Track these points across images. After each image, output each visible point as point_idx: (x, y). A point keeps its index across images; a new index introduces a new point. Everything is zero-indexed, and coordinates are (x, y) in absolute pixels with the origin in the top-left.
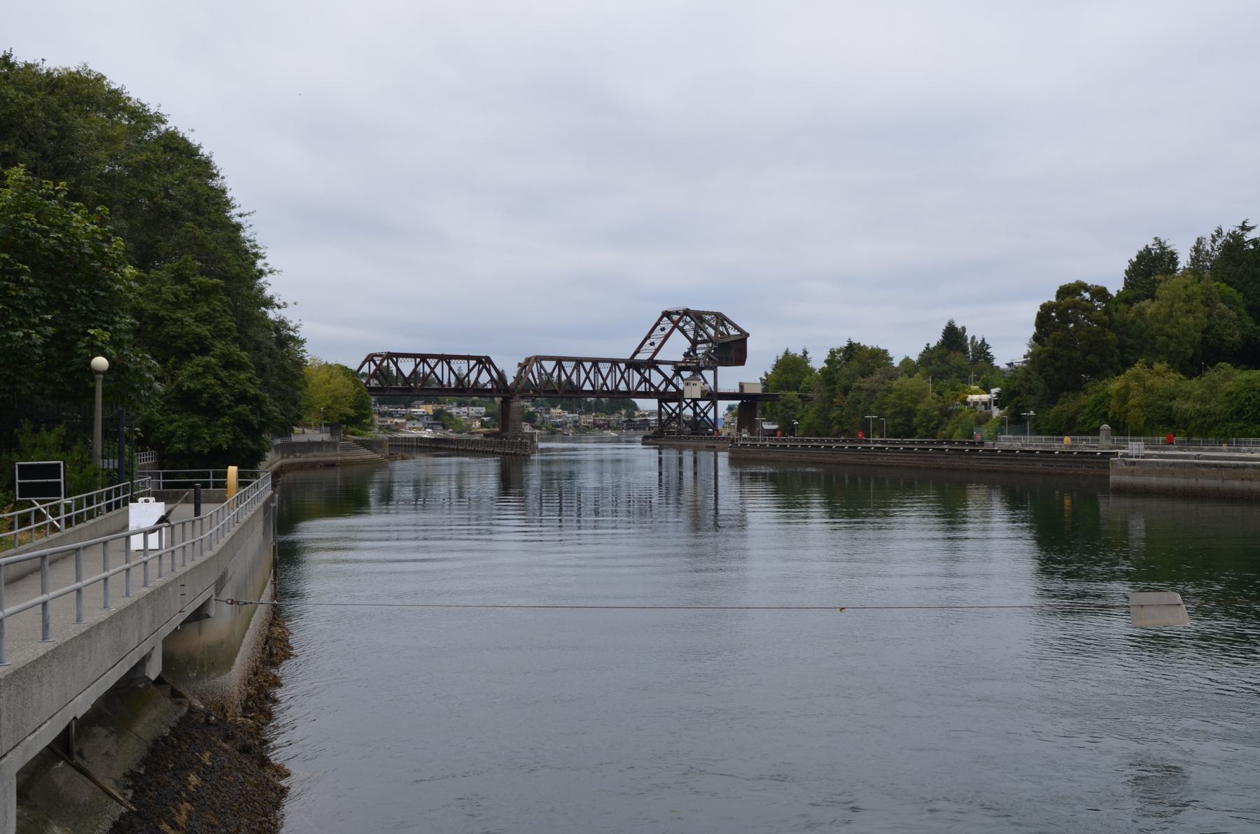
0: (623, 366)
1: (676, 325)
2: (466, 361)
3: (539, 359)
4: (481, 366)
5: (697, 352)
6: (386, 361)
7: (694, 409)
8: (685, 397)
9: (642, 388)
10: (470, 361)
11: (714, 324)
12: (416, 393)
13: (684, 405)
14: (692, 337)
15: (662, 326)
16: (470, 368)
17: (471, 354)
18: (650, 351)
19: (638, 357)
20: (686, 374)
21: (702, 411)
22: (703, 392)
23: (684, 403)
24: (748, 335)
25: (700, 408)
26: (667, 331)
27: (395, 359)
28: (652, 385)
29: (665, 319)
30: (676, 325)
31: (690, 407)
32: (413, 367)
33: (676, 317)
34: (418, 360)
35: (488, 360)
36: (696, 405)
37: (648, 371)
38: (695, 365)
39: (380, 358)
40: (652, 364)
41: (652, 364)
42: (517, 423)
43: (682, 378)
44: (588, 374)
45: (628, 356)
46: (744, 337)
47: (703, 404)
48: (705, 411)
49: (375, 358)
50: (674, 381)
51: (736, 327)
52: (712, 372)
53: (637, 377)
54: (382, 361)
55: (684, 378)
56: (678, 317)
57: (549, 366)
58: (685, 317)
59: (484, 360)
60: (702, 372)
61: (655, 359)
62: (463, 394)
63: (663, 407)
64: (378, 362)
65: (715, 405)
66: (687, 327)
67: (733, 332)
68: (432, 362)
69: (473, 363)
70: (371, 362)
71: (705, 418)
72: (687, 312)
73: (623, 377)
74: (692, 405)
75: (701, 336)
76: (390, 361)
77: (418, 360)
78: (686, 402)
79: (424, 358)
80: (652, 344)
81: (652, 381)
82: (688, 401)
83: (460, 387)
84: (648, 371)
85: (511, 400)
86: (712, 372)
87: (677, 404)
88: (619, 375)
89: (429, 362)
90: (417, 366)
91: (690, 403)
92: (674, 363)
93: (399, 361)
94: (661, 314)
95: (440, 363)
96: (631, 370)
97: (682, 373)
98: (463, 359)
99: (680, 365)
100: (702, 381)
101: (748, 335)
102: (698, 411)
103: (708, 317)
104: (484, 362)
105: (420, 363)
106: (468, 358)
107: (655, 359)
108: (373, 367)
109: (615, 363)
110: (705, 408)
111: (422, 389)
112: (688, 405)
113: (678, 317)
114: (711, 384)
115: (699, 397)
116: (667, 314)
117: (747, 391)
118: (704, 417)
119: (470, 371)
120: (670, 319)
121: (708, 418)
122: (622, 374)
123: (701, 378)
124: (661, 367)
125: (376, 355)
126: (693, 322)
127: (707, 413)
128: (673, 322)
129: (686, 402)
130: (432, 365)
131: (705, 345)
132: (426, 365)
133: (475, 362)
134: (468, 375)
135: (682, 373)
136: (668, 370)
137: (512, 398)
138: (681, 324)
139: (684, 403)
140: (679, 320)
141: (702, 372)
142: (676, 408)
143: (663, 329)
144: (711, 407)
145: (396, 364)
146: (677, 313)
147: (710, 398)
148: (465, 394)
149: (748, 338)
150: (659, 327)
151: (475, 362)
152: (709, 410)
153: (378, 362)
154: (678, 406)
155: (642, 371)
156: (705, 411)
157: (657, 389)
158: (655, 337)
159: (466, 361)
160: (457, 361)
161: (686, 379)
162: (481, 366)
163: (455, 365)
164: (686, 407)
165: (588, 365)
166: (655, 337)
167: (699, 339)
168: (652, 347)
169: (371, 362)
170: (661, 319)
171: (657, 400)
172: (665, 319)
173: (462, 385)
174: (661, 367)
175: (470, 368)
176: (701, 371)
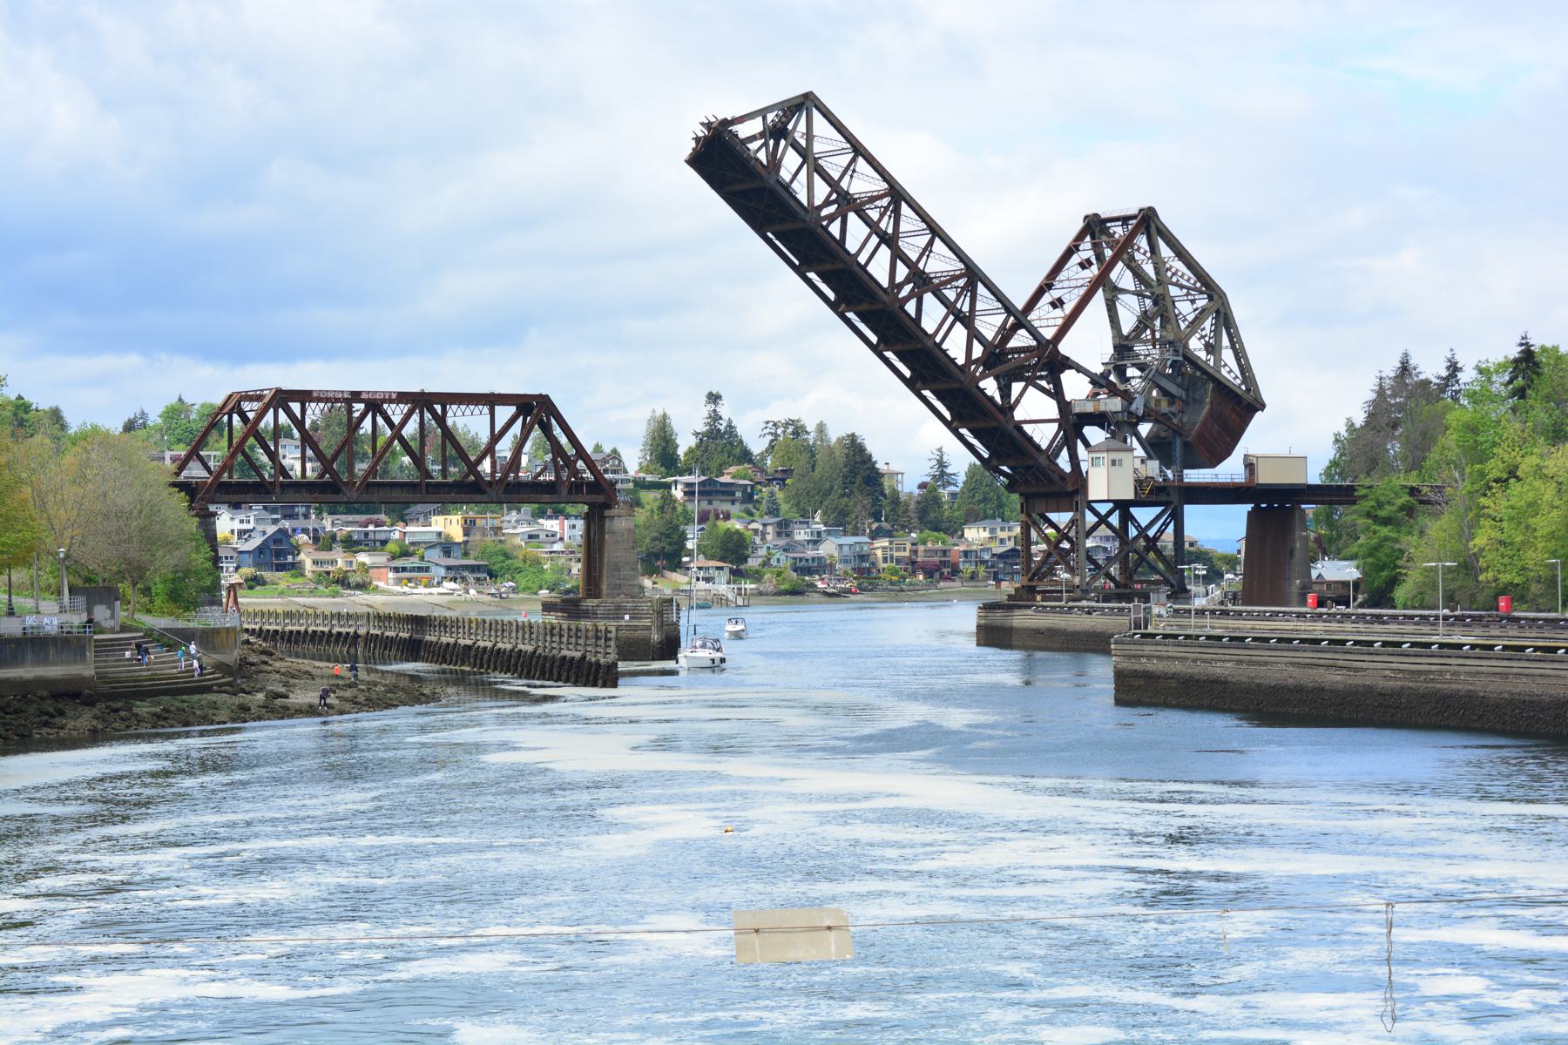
6: (270, 415)
7: (1121, 533)
8: (1091, 497)
10: (497, 408)
12: (353, 495)
16: (498, 429)
17: (497, 391)
21: (1142, 531)
22: (1139, 483)
23: (1088, 513)
25: (1138, 526)
36: (1126, 518)
39: (256, 405)
42: (626, 572)
43: (1087, 444)
47: (1143, 515)
48: (1151, 533)
49: (246, 406)
54: (261, 414)
55: (1092, 443)
62: (478, 497)
65: (1177, 518)
69: (504, 413)
71: (1152, 555)
74: (1114, 520)
76: (280, 410)
78: (1096, 513)
82: (1103, 509)
83: (472, 478)
85: (607, 513)
89: (389, 412)
91: (1110, 513)
94: (1080, 225)
106: (491, 400)
111: (368, 486)
115: (1130, 495)
117: (1265, 477)
118: (1147, 549)
121: (1159, 553)
130: (396, 420)
133: (512, 410)
137: (609, 507)
144: (1166, 524)
147: (1163, 498)
148: (485, 498)
151: (512, 410)
152: (1161, 531)
154: (1073, 522)
156: (1151, 533)
159: (486, 410)
160: (472, 407)
173: (478, 475)
175: (498, 429)
176: (1137, 424)
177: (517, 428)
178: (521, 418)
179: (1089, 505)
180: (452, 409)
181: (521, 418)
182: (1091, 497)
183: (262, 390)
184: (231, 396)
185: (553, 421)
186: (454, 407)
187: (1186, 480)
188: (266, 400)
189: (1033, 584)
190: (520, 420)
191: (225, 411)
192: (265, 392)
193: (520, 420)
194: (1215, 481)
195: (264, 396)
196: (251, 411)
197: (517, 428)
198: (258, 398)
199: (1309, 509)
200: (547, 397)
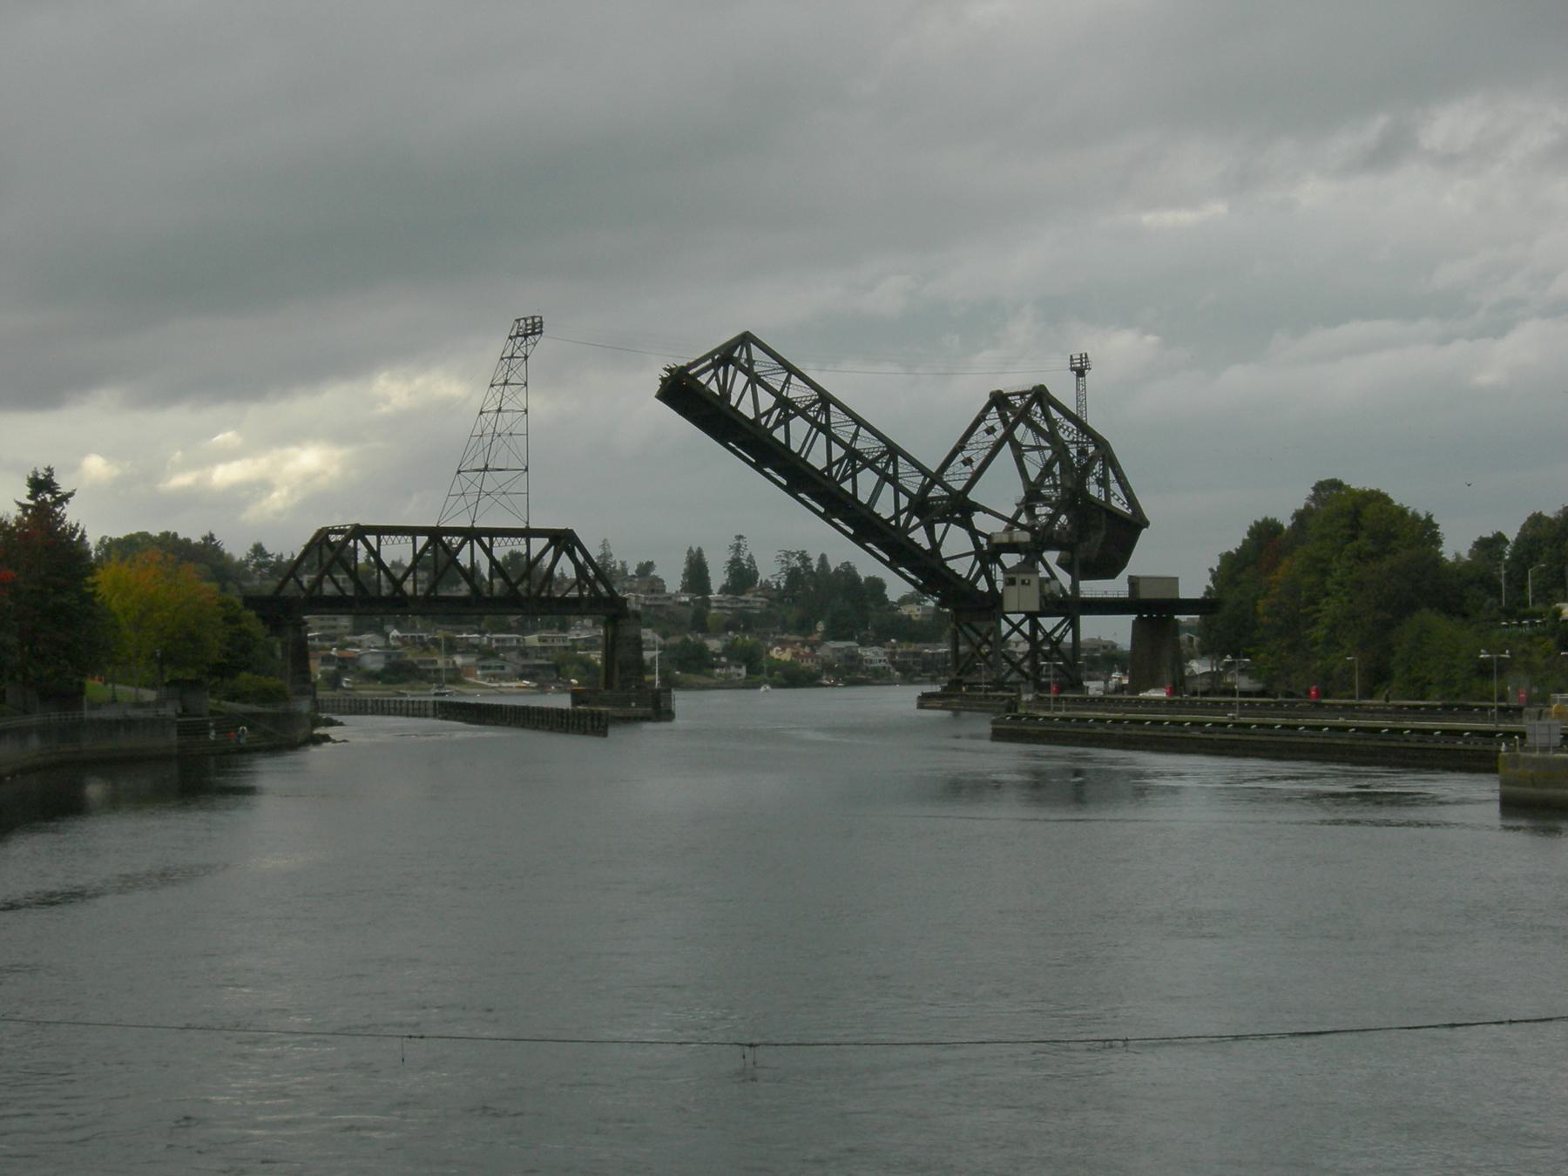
7: (1031, 639)
8: (1006, 609)
20: (1011, 560)
22: (1043, 597)
36: (1035, 626)
47: (1048, 623)
65: (1075, 625)
74: (1026, 628)
76: (359, 541)
82: (1016, 619)
91: (1022, 622)
98: (516, 537)
104: (563, 540)
144: (1066, 631)
151: (546, 541)
152: (1062, 636)
161: (1012, 570)
180: (498, 540)
185: (576, 548)
186: (499, 539)
187: (1082, 596)
189: (961, 677)
190: (553, 548)
194: (1105, 596)
200: (572, 530)
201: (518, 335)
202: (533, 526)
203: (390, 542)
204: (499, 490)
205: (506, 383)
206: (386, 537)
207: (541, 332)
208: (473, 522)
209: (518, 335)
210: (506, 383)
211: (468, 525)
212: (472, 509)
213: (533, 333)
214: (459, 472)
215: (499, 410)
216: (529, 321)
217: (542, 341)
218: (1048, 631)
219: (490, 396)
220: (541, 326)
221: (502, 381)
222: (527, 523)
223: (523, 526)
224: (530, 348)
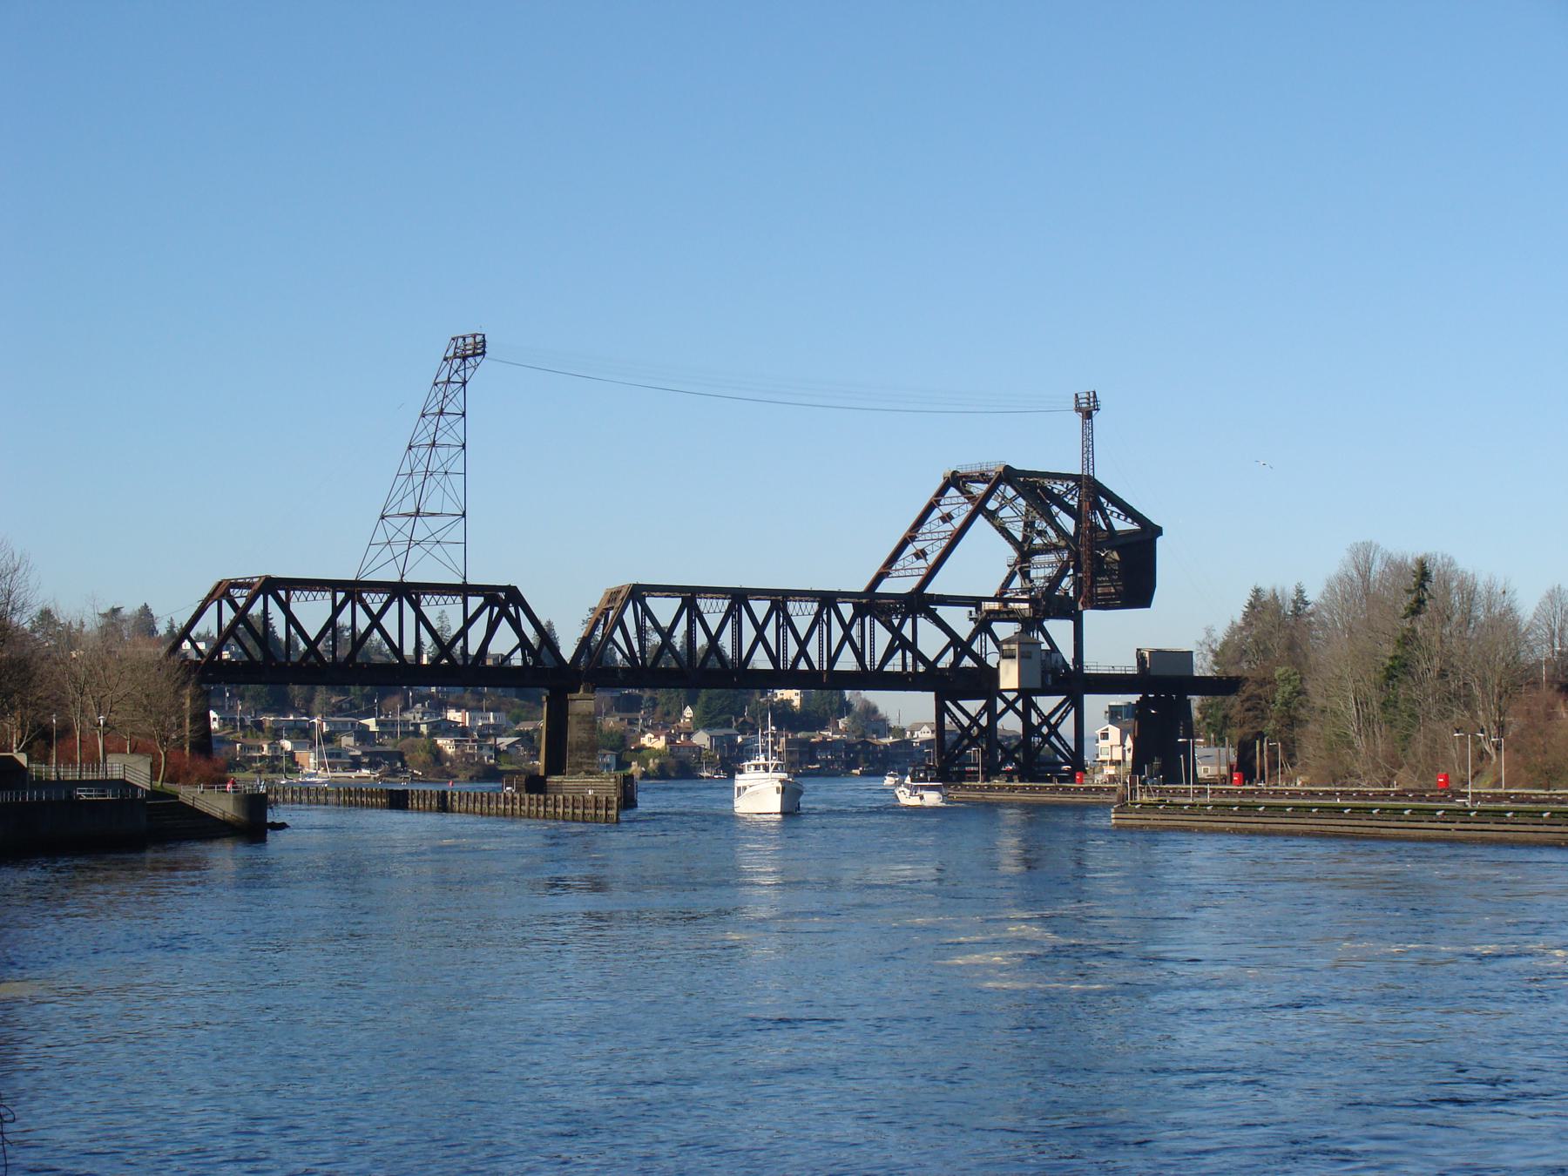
0: (847, 610)
1: (980, 508)
2: (459, 599)
3: (638, 593)
4: (496, 610)
5: (1033, 574)
7: (1025, 716)
8: (1002, 687)
9: (895, 665)
11: (1074, 503)
13: (1000, 705)
14: (1019, 537)
15: (946, 510)
16: (470, 615)
18: (916, 572)
19: (885, 587)
20: (1005, 630)
21: (1045, 720)
23: (999, 701)
24: (1158, 531)
25: (1040, 714)
26: (957, 522)
27: (282, 594)
28: (919, 657)
29: (952, 492)
30: (980, 508)
31: (1016, 711)
32: (330, 613)
33: (979, 489)
34: (340, 596)
35: (514, 595)
36: (1030, 705)
37: (909, 622)
38: (1026, 606)
39: (246, 592)
40: (920, 603)
41: (920, 603)
44: (760, 629)
45: (861, 587)
46: (1150, 532)
47: (1047, 703)
48: (1053, 721)
49: (235, 592)
50: (976, 647)
51: (1129, 512)
52: (1069, 624)
53: (883, 637)
54: (250, 602)
56: (985, 487)
57: (664, 609)
58: (1002, 487)
59: (502, 595)
60: (1045, 623)
61: (929, 590)
63: (948, 710)
64: (241, 602)
66: (1006, 513)
67: (1122, 525)
68: (375, 601)
69: (475, 602)
70: (225, 603)
72: (1009, 475)
73: (847, 637)
74: (1019, 705)
75: (1041, 533)
76: (269, 596)
77: (340, 596)
78: (1005, 700)
79: (353, 590)
80: (921, 554)
81: (920, 647)
82: (1011, 696)
84: (909, 622)
86: (1069, 624)
87: (982, 703)
88: (837, 633)
89: (368, 601)
90: (337, 610)
91: (1016, 700)
92: (976, 602)
93: (294, 599)
95: (395, 605)
96: (867, 619)
97: (996, 626)
99: (987, 606)
100: (1045, 646)
101: (1158, 531)
102: (1035, 719)
103: (1058, 488)
105: (344, 603)
106: (464, 590)
107: (929, 590)
108: (229, 615)
109: (828, 601)
110: (1052, 714)
112: (1010, 705)
113: (985, 487)
114: (1068, 655)
115: (1037, 684)
116: (956, 481)
118: (1049, 734)
119: (468, 622)
120: (964, 492)
121: (1059, 737)
122: (847, 628)
123: (1041, 638)
124: (943, 611)
125: (236, 585)
126: (1021, 501)
127: (1057, 725)
128: (970, 497)
129: (1005, 700)
130: (375, 609)
131: (1052, 557)
132: (359, 608)
133: (480, 600)
134: (463, 633)
135: (996, 626)
136: (961, 621)
138: (992, 505)
139: (999, 701)
140: (988, 496)
141: (1045, 623)
142: (980, 714)
143: (947, 518)
144: (1067, 712)
145: (285, 606)
146: (982, 478)
149: (1159, 540)
150: (936, 513)
151: (480, 600)
152: (1062, 718)
153: (241, 602)
154: (984, 708)
155: (896, 622)
156: (1053, 721)
157: (931, 665)
158: (928, 536)
159: (459, 599)
162: (496, 610)
163: (433, 608)
164: (1004, 711)
165: (761, 608)
166: (928, 536)
167: (1038, 541)
168: (922, 563)
169: (225, 603)
170: (942, 492)
171: (932, 694)
172: (952, 492)
174: (943, 611)
175: (470, 615)
177: (483, 619)
178: (488, 608)
179: (1000, 693)
181: (488, 608)
182: (1002, 687)
183: (252, 578)
184: (220, 583)
186: (428, 597)
187: (1086, 672)
188: (256, 587)
190: (487, 610)
191: (216, 597)
192: (255, 580)
193: (487, 610)
194: (1112, 672)
195: (254, 584)
196: (241, 597)
197: (483, 619)
198: (248, 586)
199: (1195, 701)
201: (455, 356)
202: (470, 581)
203: (302, 598)
204: (432, 539)
205: (441, 413)
206: (298, 593)
207: (483, 353)
208: (403, 575)
209: (455, 356)
210: (441, 413)
211: (396, 579)
212: (401, 560)
213: (474, 355)
214: (383, 517)
215: (434, 444)
216: (470, 340)
217: (485, 363)
218: (1046, 714)
219: (421, 426)
220: (484, 346)
221: (437, 410)
222: (465, 578)
223: (459, 581)
224: (469, 372)
